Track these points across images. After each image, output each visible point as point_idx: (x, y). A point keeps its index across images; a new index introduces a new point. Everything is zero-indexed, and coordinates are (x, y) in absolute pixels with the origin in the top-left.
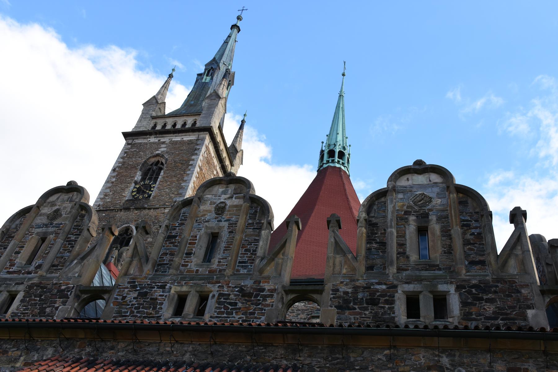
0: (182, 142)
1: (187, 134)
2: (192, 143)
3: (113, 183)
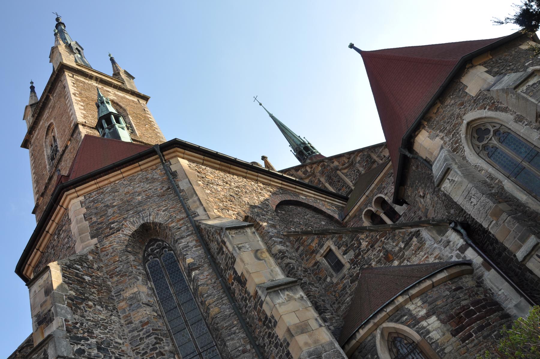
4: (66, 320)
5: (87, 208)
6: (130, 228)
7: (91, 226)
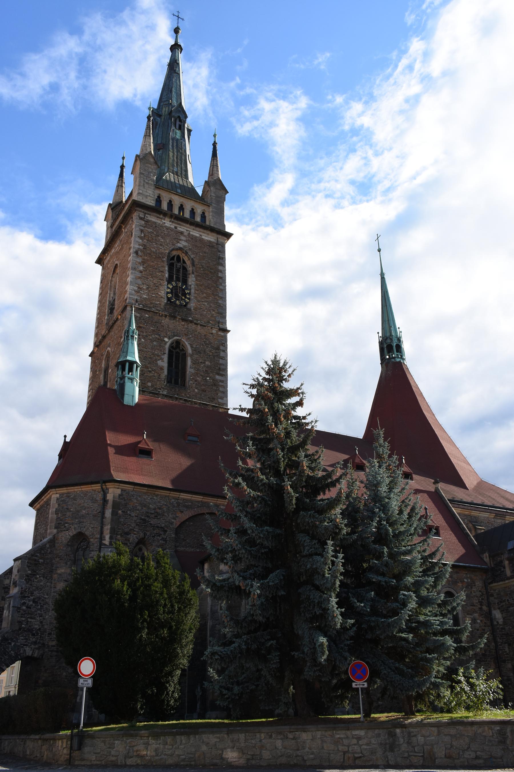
0: (201, 240)
1: (205, 231)
2: (213, 247)
3: (141, 272)
4: (22, 588)
5: (59, 505)
6: (72, 532)
7: (58, 518)
